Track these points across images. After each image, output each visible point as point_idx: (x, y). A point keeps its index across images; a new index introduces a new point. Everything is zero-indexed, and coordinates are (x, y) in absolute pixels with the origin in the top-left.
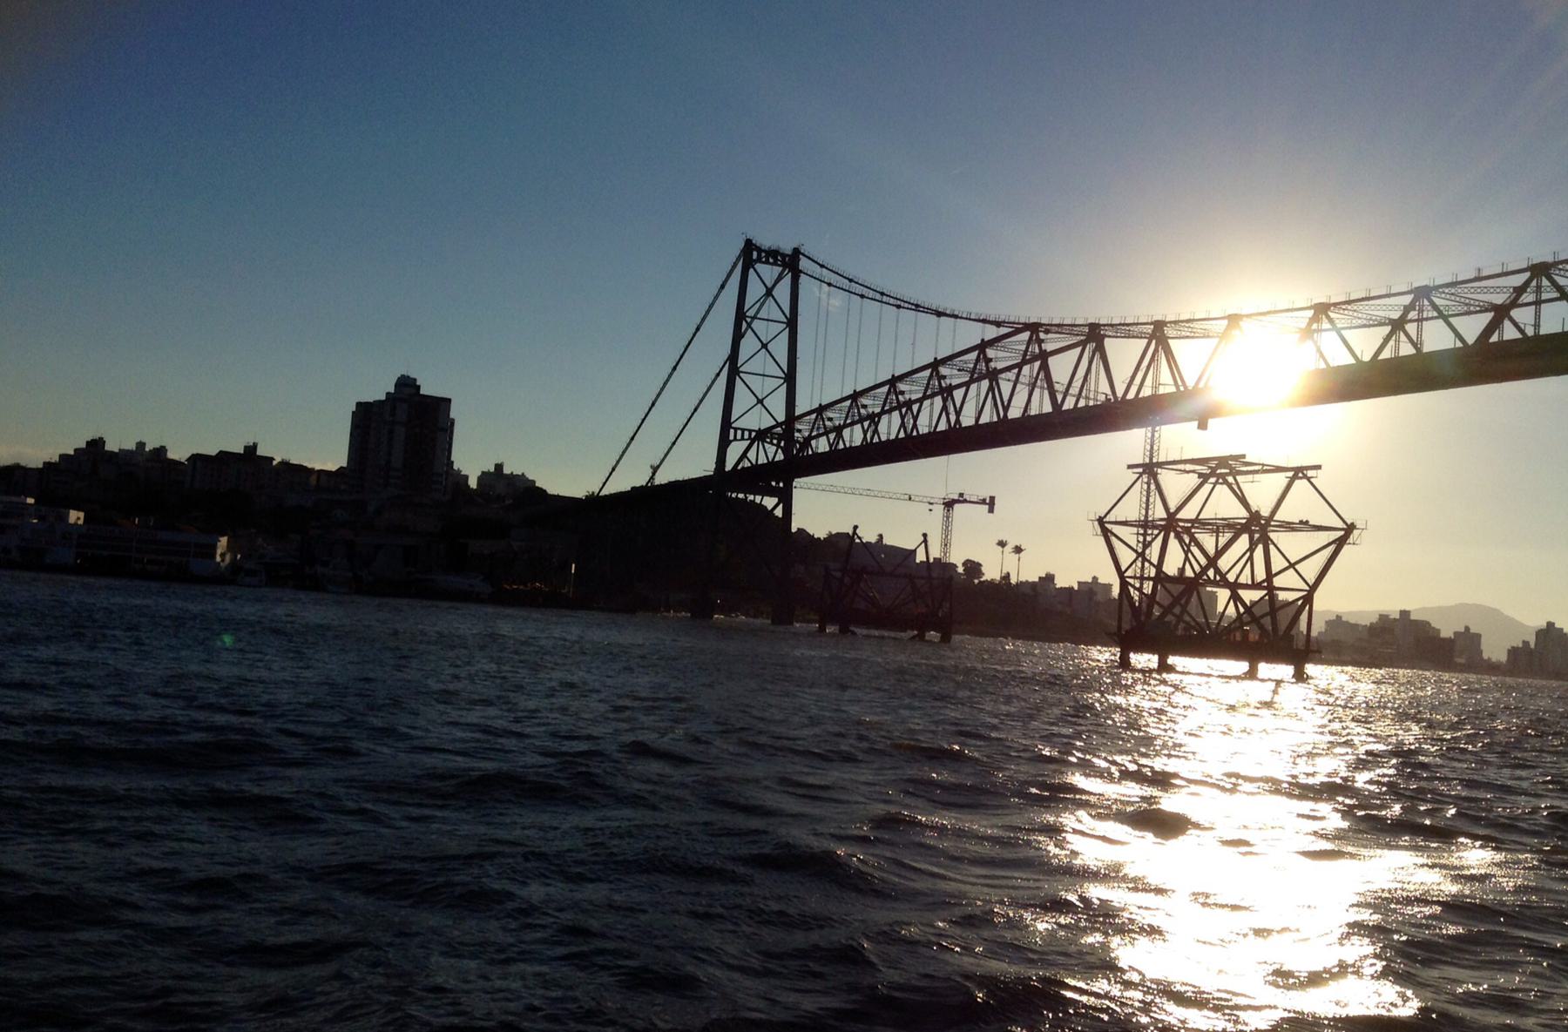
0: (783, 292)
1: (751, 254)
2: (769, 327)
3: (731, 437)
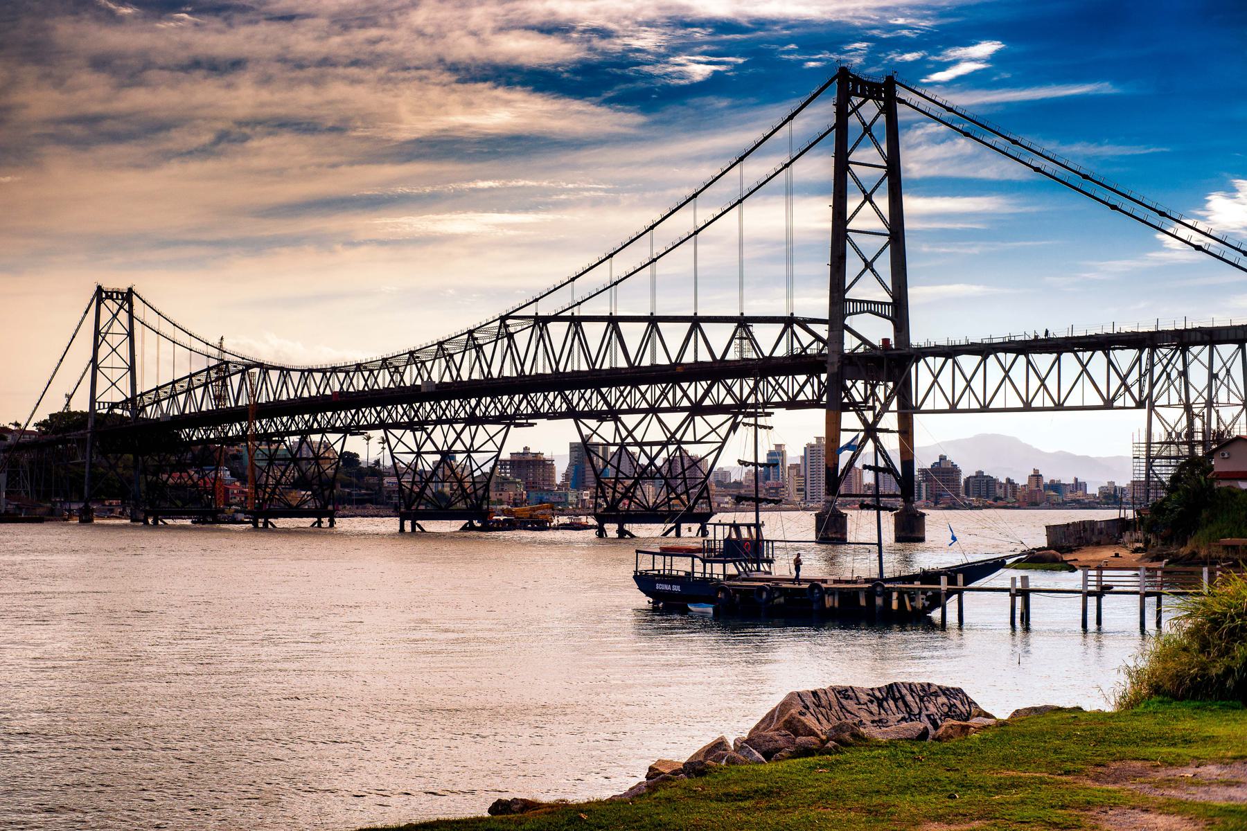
0: (123, 316)
1: (101, 295)
2: (116, 337)
3: (97, 408)
